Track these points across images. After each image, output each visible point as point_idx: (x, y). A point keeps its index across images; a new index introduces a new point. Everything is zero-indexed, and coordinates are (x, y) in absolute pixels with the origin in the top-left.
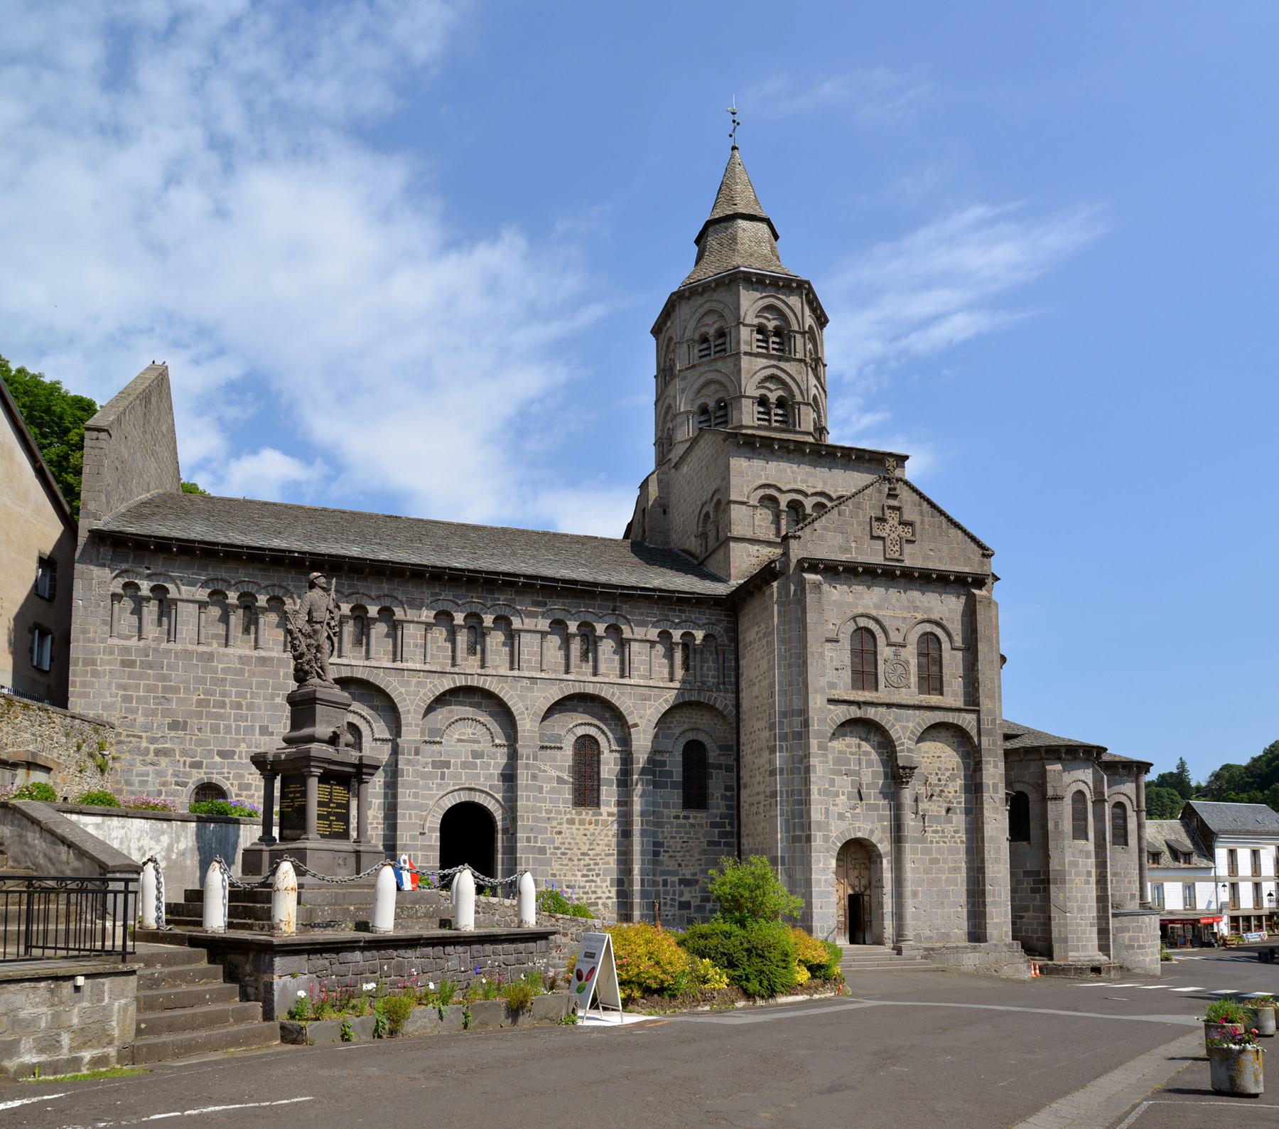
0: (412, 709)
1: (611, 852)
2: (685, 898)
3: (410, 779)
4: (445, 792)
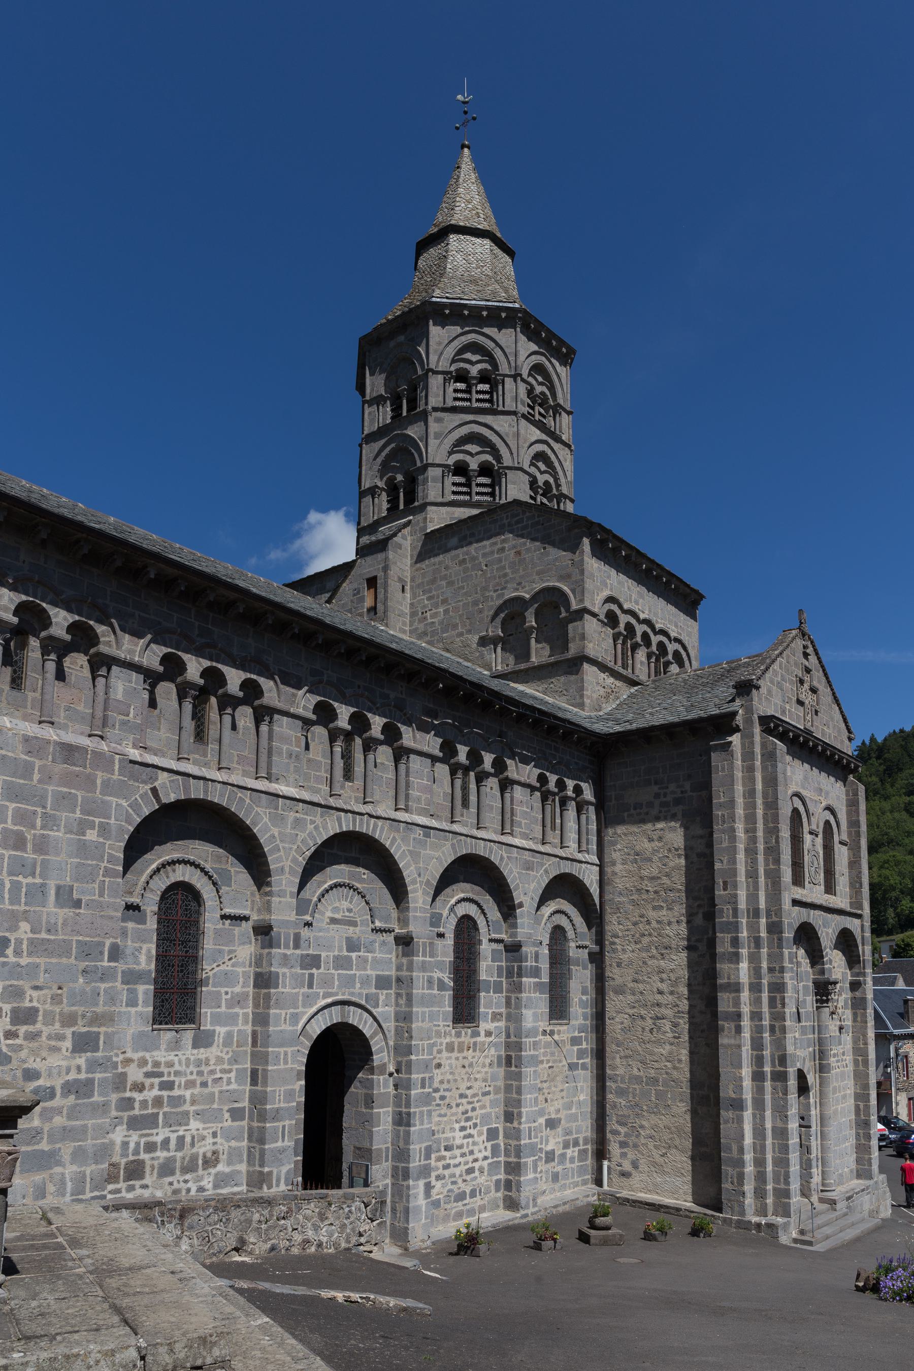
0: (287, 864)
1: (487, 1089)
2: (549, 1148)
3: (287, 990)
4: (314, 1009)
